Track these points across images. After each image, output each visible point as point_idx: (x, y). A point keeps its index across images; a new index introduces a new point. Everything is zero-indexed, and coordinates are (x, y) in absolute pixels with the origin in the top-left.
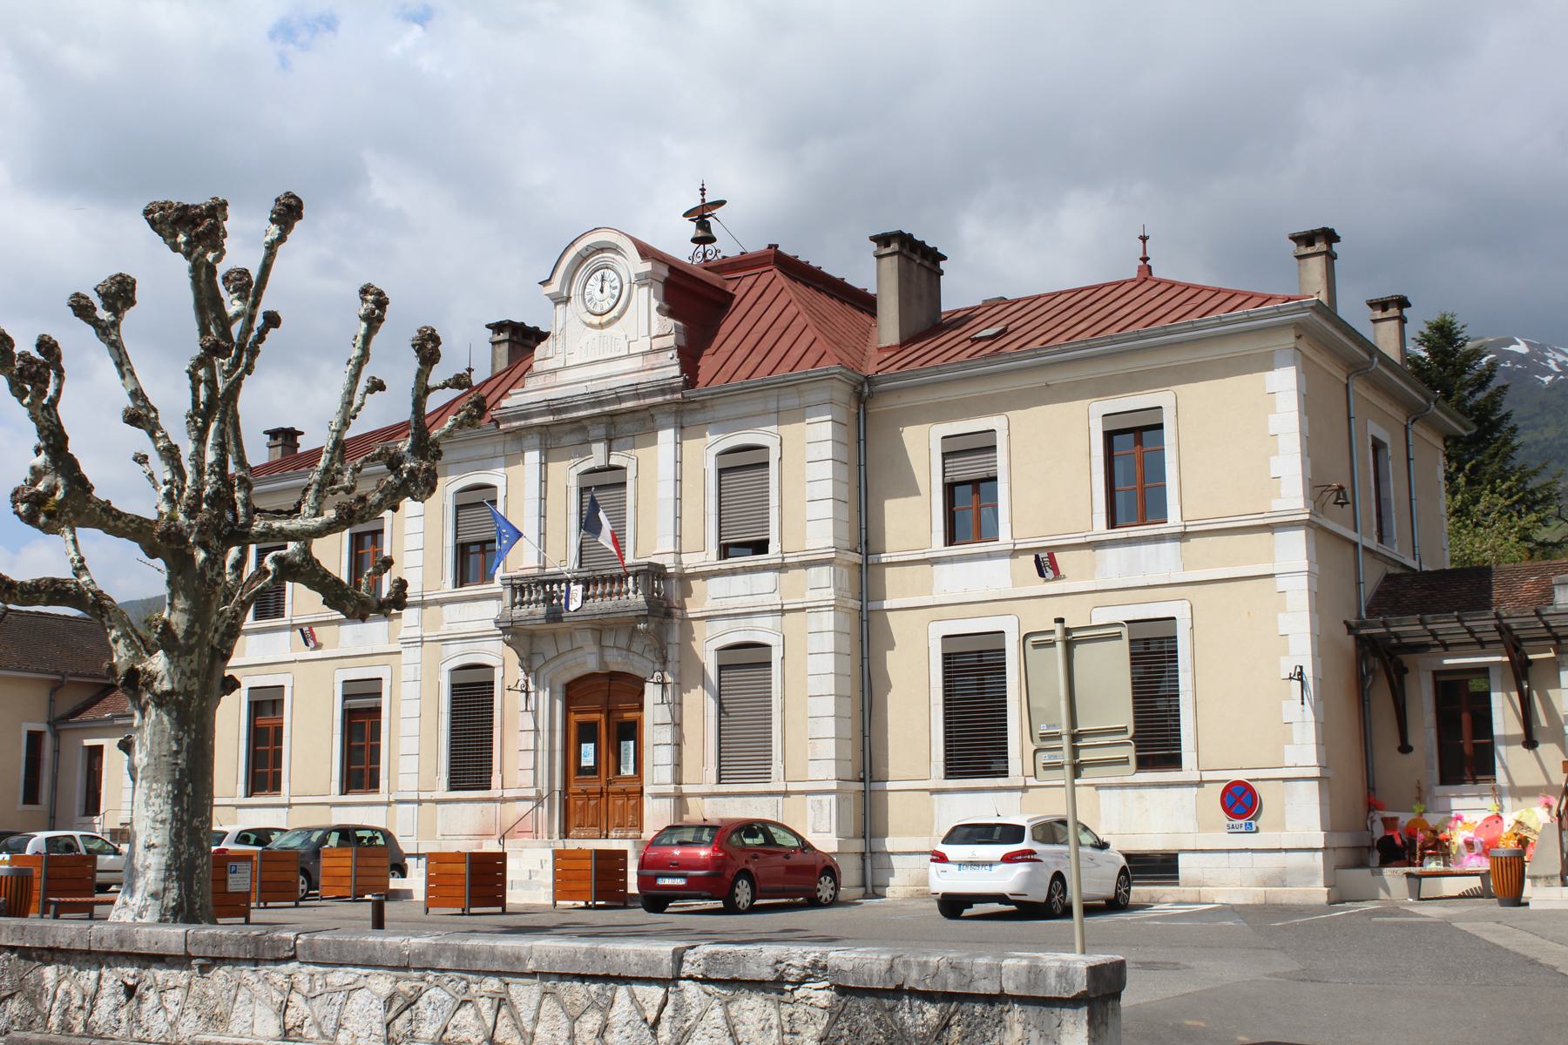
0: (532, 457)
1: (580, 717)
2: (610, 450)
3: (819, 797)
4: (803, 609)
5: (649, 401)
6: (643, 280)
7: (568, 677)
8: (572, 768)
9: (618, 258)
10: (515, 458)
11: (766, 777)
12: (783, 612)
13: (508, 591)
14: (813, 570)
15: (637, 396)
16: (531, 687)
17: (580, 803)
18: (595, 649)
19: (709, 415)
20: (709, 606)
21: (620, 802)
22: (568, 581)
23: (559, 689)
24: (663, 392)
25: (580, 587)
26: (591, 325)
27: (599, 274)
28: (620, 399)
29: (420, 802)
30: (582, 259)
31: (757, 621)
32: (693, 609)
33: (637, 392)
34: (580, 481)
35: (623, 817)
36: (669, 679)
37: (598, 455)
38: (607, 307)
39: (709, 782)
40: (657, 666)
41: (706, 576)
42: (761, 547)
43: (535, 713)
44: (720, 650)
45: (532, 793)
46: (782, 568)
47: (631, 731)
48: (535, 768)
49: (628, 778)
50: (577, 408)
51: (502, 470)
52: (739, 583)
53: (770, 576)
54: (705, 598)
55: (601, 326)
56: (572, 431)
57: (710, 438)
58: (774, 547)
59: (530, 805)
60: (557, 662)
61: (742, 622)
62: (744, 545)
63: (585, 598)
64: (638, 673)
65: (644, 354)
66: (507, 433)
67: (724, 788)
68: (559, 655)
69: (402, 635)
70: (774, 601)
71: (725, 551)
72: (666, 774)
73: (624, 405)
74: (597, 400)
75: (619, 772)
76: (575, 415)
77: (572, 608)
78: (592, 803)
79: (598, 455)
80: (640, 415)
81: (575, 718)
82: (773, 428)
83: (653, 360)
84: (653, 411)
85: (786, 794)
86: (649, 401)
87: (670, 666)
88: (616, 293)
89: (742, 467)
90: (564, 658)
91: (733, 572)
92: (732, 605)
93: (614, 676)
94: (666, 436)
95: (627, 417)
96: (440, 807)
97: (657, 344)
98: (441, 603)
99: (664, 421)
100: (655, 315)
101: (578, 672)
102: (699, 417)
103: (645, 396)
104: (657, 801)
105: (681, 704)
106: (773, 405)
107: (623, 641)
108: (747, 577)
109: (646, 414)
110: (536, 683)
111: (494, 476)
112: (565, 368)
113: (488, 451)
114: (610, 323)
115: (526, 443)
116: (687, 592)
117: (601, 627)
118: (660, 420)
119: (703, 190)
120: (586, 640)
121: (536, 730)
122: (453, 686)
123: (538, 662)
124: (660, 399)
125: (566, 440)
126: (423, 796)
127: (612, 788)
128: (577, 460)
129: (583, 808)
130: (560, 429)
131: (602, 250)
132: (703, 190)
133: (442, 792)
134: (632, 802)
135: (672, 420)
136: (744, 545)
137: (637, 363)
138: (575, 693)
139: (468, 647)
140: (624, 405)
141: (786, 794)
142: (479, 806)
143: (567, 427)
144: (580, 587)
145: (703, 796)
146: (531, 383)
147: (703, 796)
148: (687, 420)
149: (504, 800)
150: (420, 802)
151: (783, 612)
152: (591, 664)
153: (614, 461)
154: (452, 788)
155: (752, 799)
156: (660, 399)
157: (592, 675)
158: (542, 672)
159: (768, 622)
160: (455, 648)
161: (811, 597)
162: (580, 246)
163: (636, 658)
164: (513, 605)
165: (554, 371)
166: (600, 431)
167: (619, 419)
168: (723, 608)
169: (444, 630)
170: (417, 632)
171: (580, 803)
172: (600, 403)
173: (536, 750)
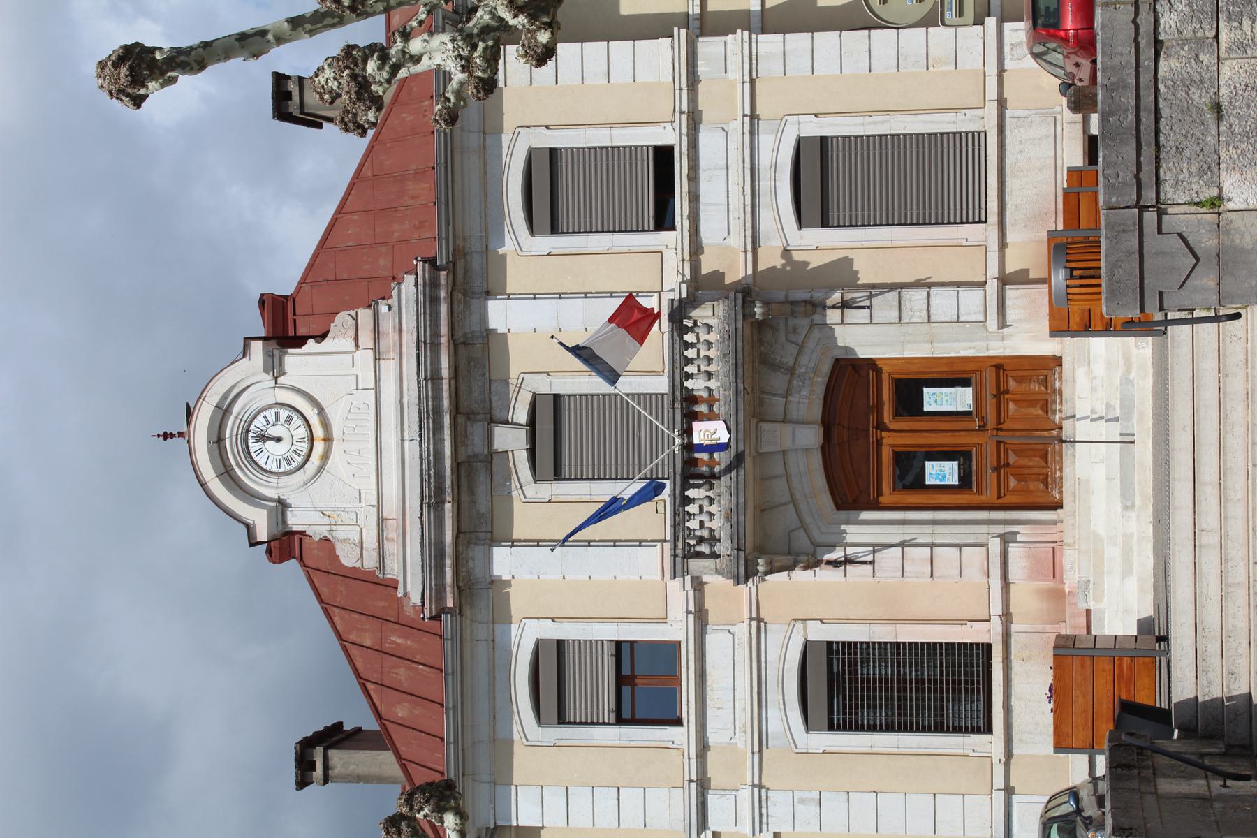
0: (503, 561)
1: (886, 487)
2: (507, 423)
3: (1007, 49)
4: (752, 82)
5: (444, 329)
6: (274, 368)
7: (826, 500)
8: (964, 495)
9: (236, 409)
10: (497, 587)
11: (977, 137)
12: (754, 117)
13: (695, 565)
14: (702, 69)
15: (435, 346)
16: (837, 554)
17: (1012, 483)
18: (788, 428)
19: (476, 246)
20: (738, 240)
21: (1012, 406)
22: (689, 447)
23: (843, 514)
24: (434, 301)
25: (697, 427)
26: (321, 468)
27: (254, 446)
28: (435, 377)
29: (1009, 791)
30: (227, 474)
31: (764, 160)
32: (738, 270)
33: (428, 344)
34: (542, 233)
35: (1032, 403)
36: (836, 297)
37: (510, 440)
38: (302, 432)
39: (987, 234)
40: (817, 318)
41: (696, 248)
42: (664, 155)
43: (877, 548)
44: (801, 225)
45: (995, 545)
46: (695, 119)
47: (908, 388)
48: (960, 546)
49: (977, 397)
50: (439, 456)
51: (514, 628)
52: (710, 189)
53: (704, 138)
54: (728, 256)
55: (328, 439)
56: (472, 491)
57: (508, 247)
58: (665, 136)
59: (1014, 550)
60: (803, 507)
61: (765, 184)
62: (660, 185)
63: (711, 417)
64: (826, 368)
65: (377, 358)
66: (460, 592)
67: (993, 218)
68: (793, 501)
69: (746, 827)
70: (737, 127)
71: (663, 220)
72: (971, 298)
73: (445, 373)
74: (431, 416)
75: (966, 414)
76: (448, 463)
77: (723, 437)
78: (1012, 459)
79: (510, 440)
80: (462, 363)
81: (886, 499)
82: (506, 139)
83: (389, 339)
84: (459, 334)
85: (1002, 104)
86: (444, 329)
87: (818, 295)
88: (284, 413)
89: (553, 192)
90: (798, 495)
91: (694, 198)
92: (738, 200)
93: (827, 423)
94: (503, 561)
95: (462, 387)
96: (1017, 751)
97: (366, 339)
98: (703, 747)
99: (475, 317)
100: (327, 345)
101: (820, 481)
102: (476, 263)
103: (436, 334)
104: (1011, 315)
105: (873, 286)
106: (473, 140)
107: (778, 381)
108: (703, 175)
109: (461, 349)
110: (832, 547)
111: (524, 638)
112: (379, 506)
113: (482, 651)
114: (326, 425)
115: (478, 572)
116: (717, 276)
117: (754, 407)
118: (472, 325)
119: (166, 436)
120: (776, 437)
121: (902, 544)
122: (831, 727)
123: (801, 541)
124: (444, 308)
125: (482, 505)
126: (999, 782)
127: (991, 422)
128: (514, 483)
129: (1020, 477)
130: (463, 495)
131: (219, 441)
132: (166, 436)
133: (991, 744)
134: (1012, 384)
135: (475, 303)
136: (660, 185)
137: (389, 368)
138: (852, 495)
139: (773, 695)
140: (445, 373)
141: (1002, 104)
142: (1016, 665)
143: (465, 498)
144: (697, 427)
145: (1003, 245)
146: (393, 570)
147: (1003, 245)
148: (477, 284)
149: (1007, 616)
150: (1009, 791)
151: (754, 117)
152: (811, 437)
153: (521, 416)
154: (988, 729)
155: (1009, 160)
156: (444, 308)
157: (826, 448)
158: (819, 538)
159: (766, 141)
160: (774, 722)
161: (736, 72)
162: (208, 473)
163: (804, 360)
164: (714, 555)
165: (381, 521)
166: (477, 430)
167: (463, 381)
168: (741, 219)
169: (744, 742)
170: (745, 795)
171: (1012, 483)
172: (437, 412)
173: (932, 546)
